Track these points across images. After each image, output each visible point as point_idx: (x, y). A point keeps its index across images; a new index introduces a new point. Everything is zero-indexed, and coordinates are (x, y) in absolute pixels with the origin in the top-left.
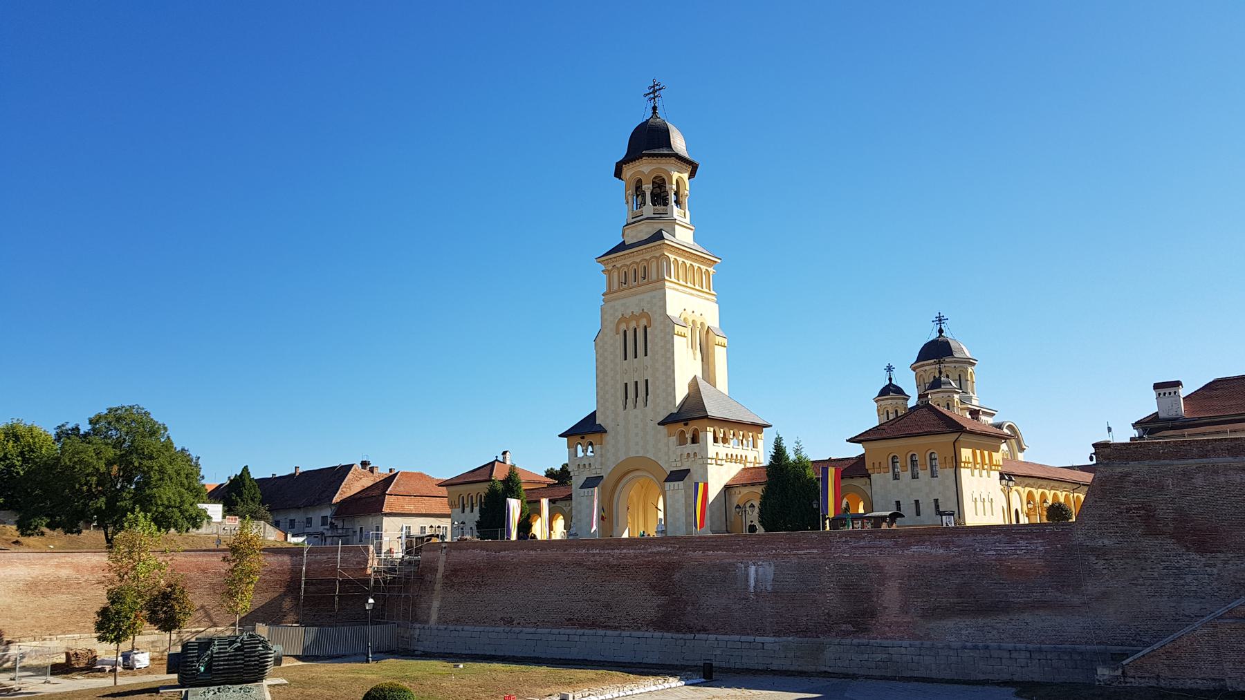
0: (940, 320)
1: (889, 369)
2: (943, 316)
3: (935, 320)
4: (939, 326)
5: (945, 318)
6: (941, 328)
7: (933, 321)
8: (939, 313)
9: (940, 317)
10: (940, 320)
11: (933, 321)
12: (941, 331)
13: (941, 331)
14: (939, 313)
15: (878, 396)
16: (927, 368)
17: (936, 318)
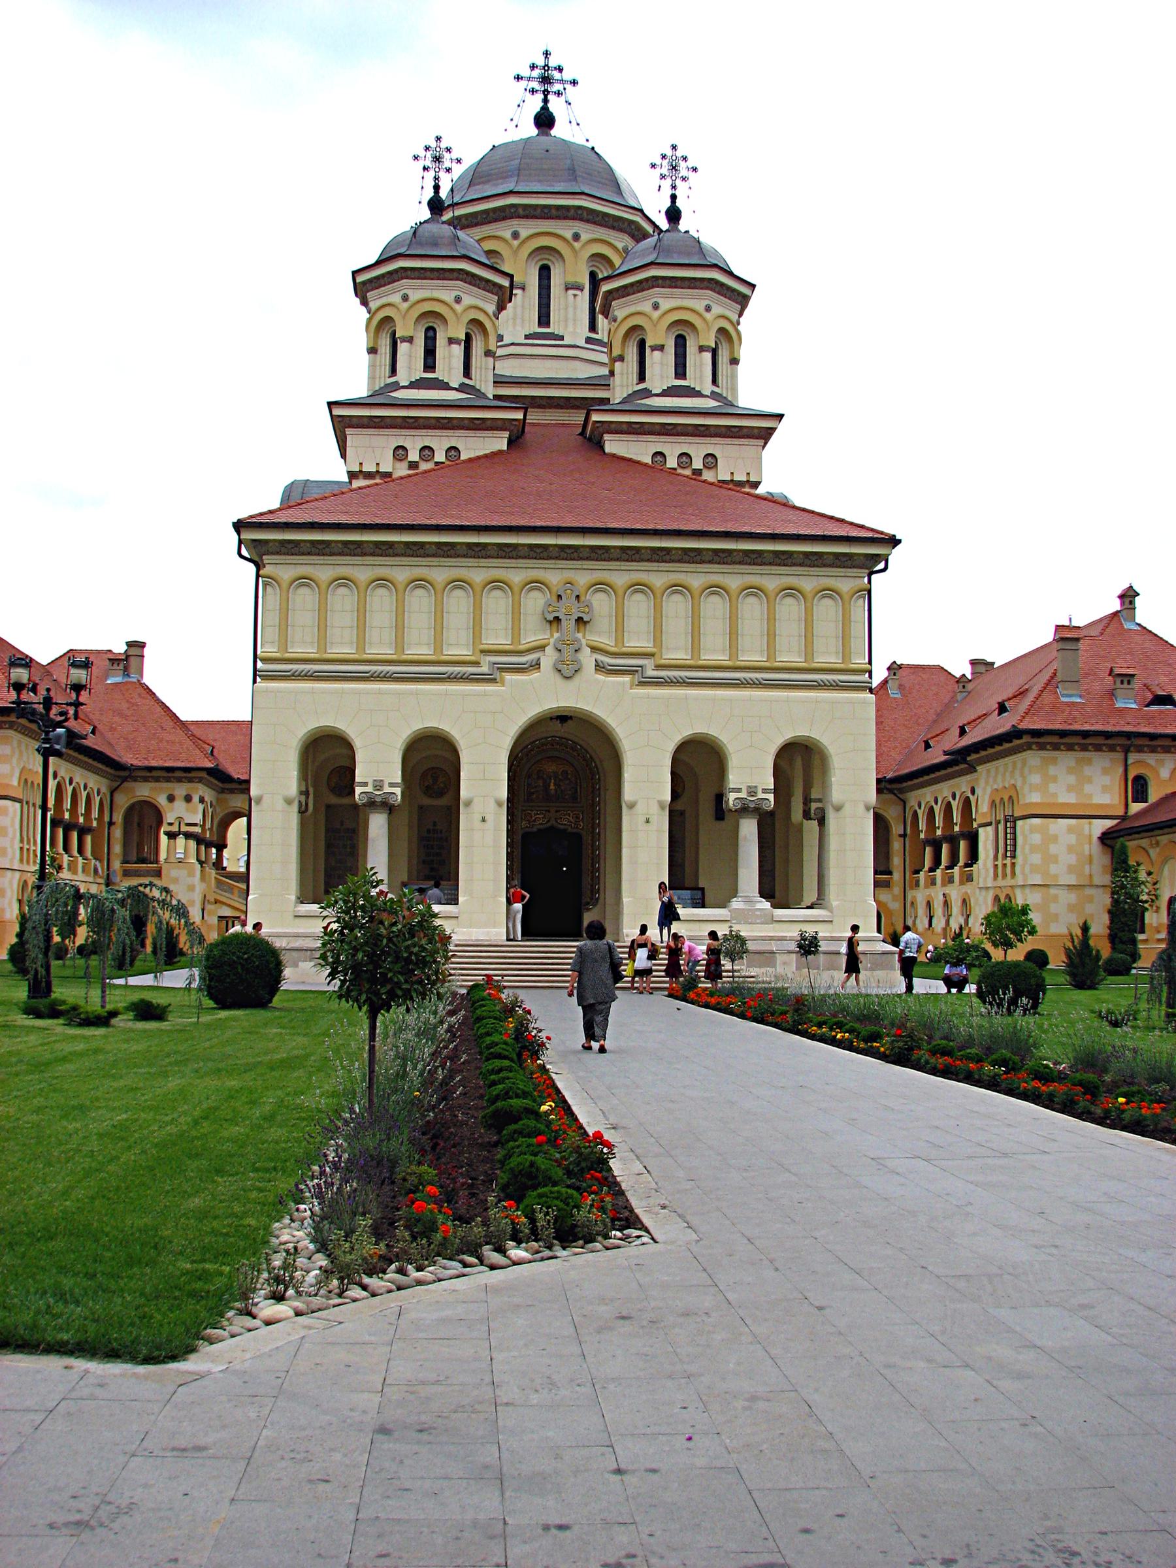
0: (546, 80)
1: (437, 159)
2: (560, 70)
3: (526, 72)
4: (535, 104)
5: (567, 75)
6: (545, 108)
7: (518, 78)
8: (547, 54)
9: (546, 67)
10: (546, 80)
11: (518, 78)
12: (545, 120)
13: (545, 120)
14: (547, 54)
15: (378, 263)
16: (526, 228)
17: (533, 67)
